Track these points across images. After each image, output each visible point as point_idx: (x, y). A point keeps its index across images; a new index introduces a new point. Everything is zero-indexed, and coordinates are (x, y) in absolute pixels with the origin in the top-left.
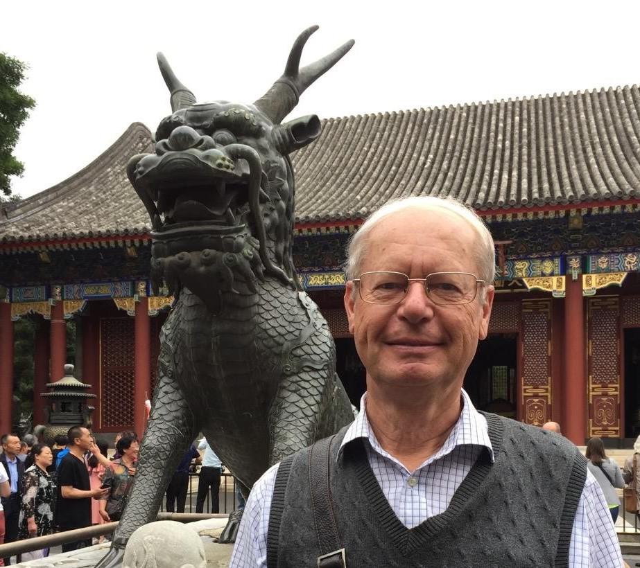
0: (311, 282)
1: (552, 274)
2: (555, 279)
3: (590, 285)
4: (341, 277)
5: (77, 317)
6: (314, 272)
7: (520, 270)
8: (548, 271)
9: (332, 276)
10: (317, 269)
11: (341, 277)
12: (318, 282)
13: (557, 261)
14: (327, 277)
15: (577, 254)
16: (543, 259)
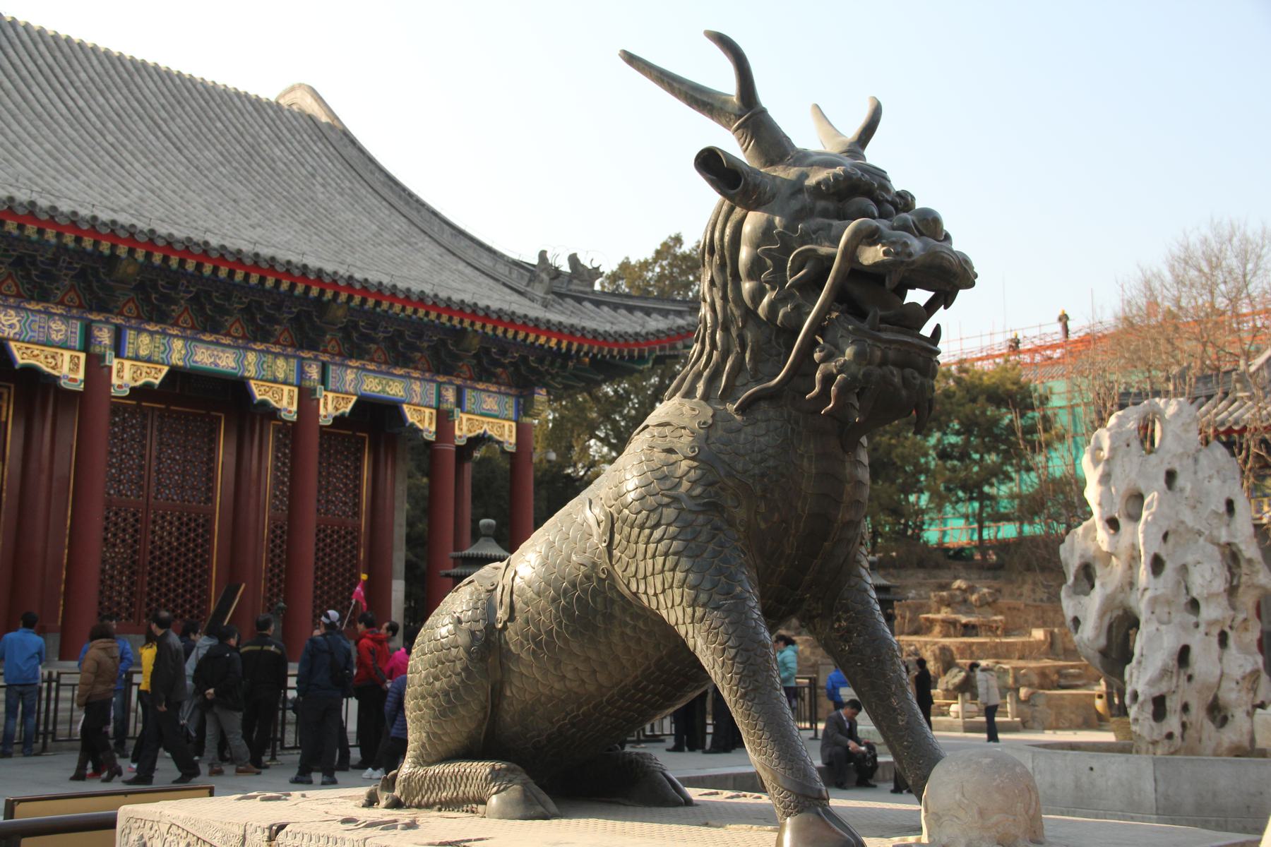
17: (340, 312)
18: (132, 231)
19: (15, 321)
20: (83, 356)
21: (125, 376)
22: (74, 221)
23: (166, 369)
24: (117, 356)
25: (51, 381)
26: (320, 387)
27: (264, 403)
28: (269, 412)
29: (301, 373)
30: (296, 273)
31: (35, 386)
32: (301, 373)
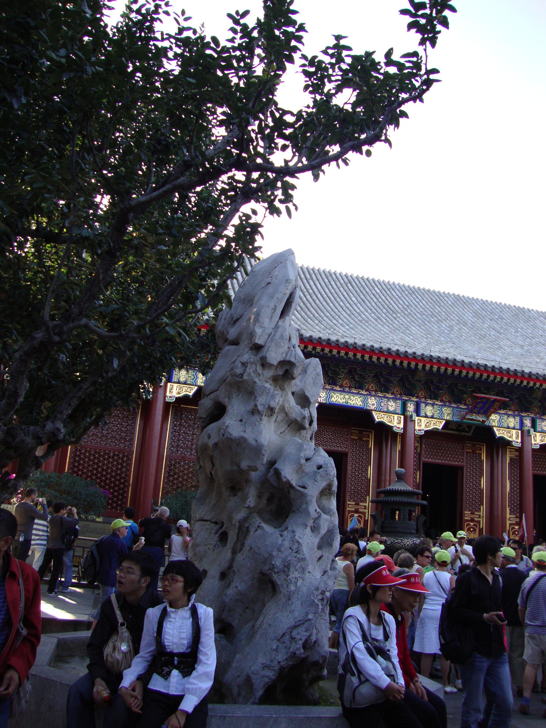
0: (333, 399)
1: (514, 428)
2: (514, 432)
3: (536, 440)
4: (359, 400)
5: (430, 434)
6: (335, 390)
7: (494, 421)
8: (511, 425)
9: (352, 397)
10: (338, 388)
11: (359, 400)
12: (339, 400)
13: (518, 419)
14: (347, 397)
15: (528, 416)
16: (509, 416)
17: (540, 393)
18: (355, 346)
19: (374, 402)
20: (402, 417)
21: (422, 425)
22: (422, 358)
23: (444, 421)
24: (417, 416)
25: (389, 429)
26: (532, 431)
27: (502, 438)
28: (505, 443)
29: (522, 424)
30: (482, 368)
31: (384, 431)
32: (522, 424)
